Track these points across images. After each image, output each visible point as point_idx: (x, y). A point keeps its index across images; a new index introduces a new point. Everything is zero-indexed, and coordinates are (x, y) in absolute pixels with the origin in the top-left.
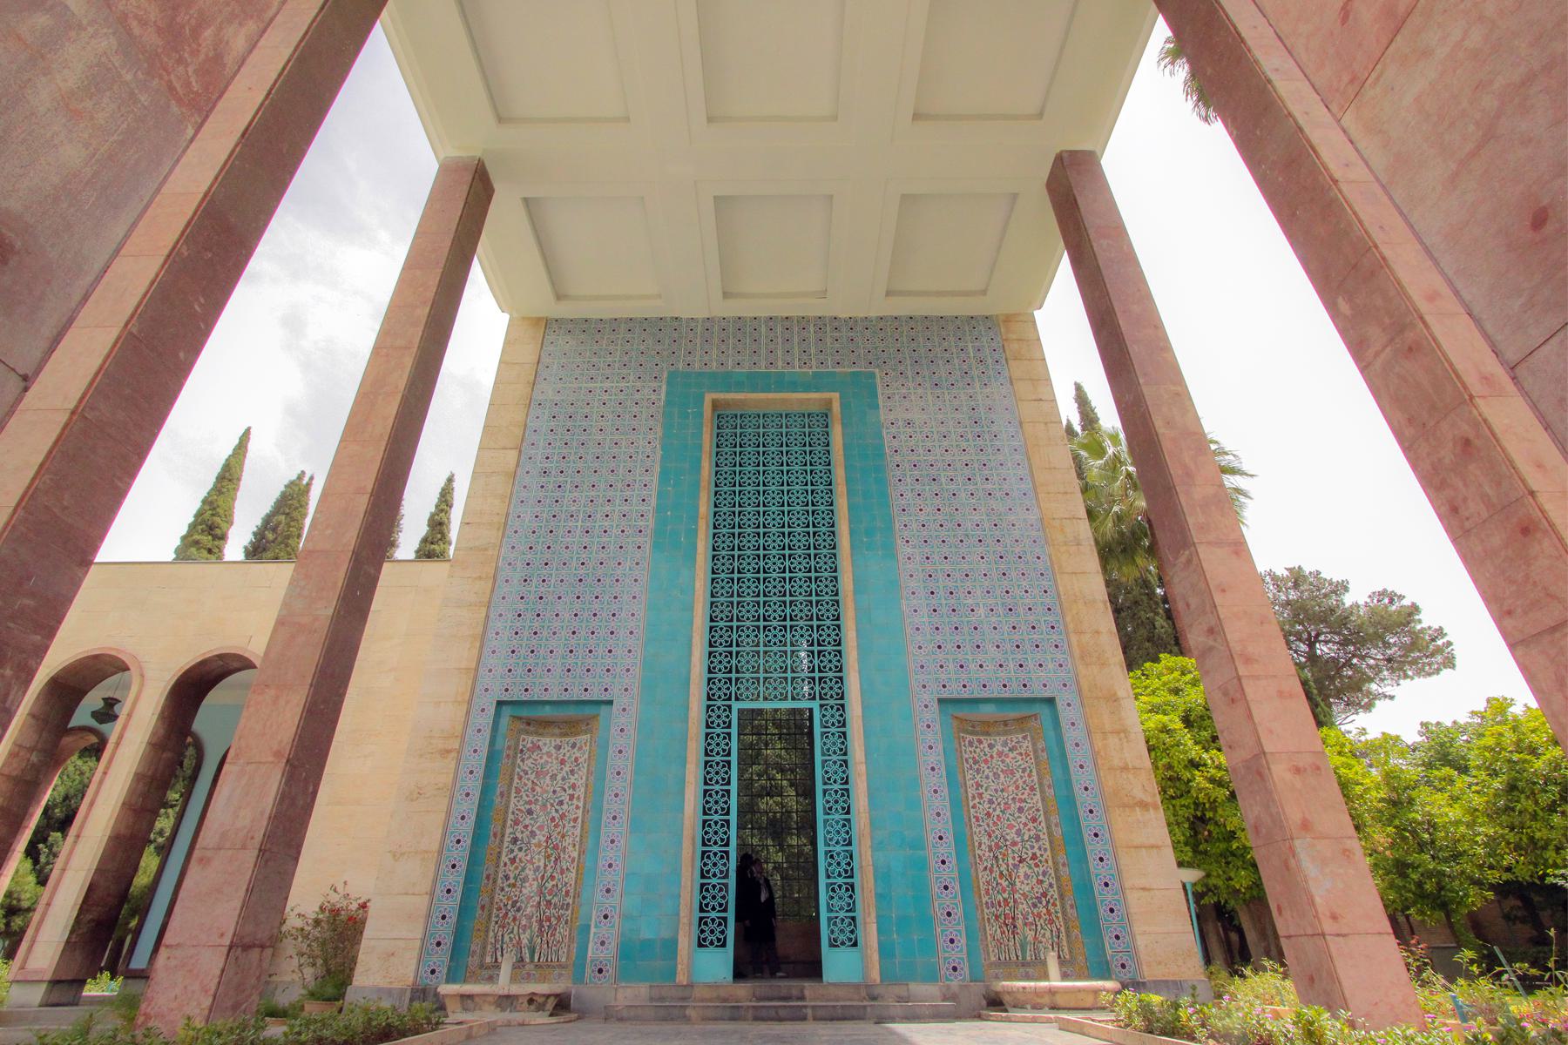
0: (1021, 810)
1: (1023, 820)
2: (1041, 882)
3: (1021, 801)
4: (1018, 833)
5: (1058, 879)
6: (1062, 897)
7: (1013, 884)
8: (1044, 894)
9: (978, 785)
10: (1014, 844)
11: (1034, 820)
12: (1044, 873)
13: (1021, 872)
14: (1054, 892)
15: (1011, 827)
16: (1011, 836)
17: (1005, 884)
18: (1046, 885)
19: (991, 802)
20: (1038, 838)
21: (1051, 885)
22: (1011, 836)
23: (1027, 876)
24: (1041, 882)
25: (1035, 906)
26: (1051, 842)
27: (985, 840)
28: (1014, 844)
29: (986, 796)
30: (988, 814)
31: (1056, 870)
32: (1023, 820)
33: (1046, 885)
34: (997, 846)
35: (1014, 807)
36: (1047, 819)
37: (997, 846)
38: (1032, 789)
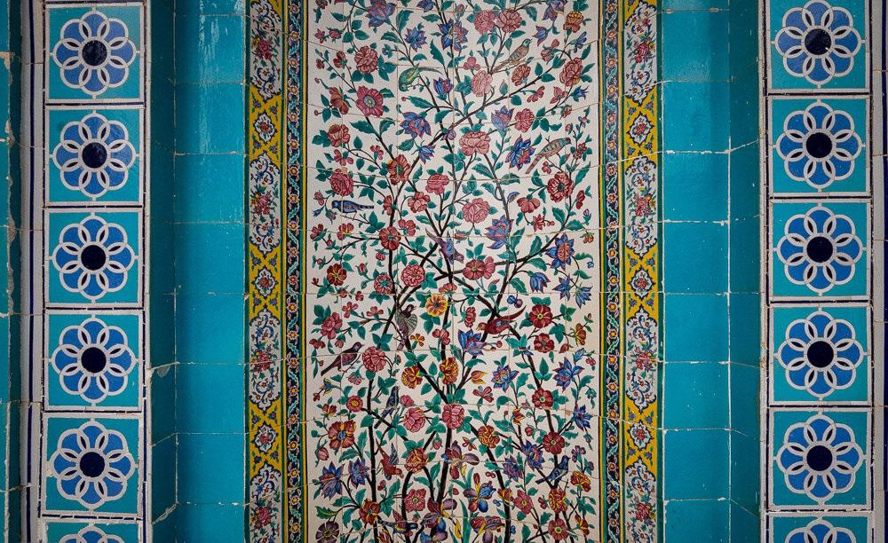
0: (521, 153)
1: (524, 187)
2: (552, 400)
3: (526, 120)
4: (500, 233)
5: (610, 401)
6: (613, 466)
7: (452, 396)
8: (554, 441)
9: (370, 64)
10: (480, 267)
11: (561, 187)
12: (564, 373)
13: (488, 363)
14: (587, 444)
15: (476, 211)
16: (474, 238)
17: (420, 397)
18: (563, 412)
19: (414, 125)
20: (561, 252)
21: (581, 417)
22: (474, 238)
23: (504, 376)
24: (552, 400)
25: (515, 470)
26: (608, 268)
27: (366, 257)
28: (480, 267)
29: (399, 105)
30: (397, 169)
31: (610, 372)
32: (524, 187)
33: (563, 412)
34: (418, 279)
35: (498, 142)
36: (608, 182)
37: (418, 279)
38: (575, 73)
